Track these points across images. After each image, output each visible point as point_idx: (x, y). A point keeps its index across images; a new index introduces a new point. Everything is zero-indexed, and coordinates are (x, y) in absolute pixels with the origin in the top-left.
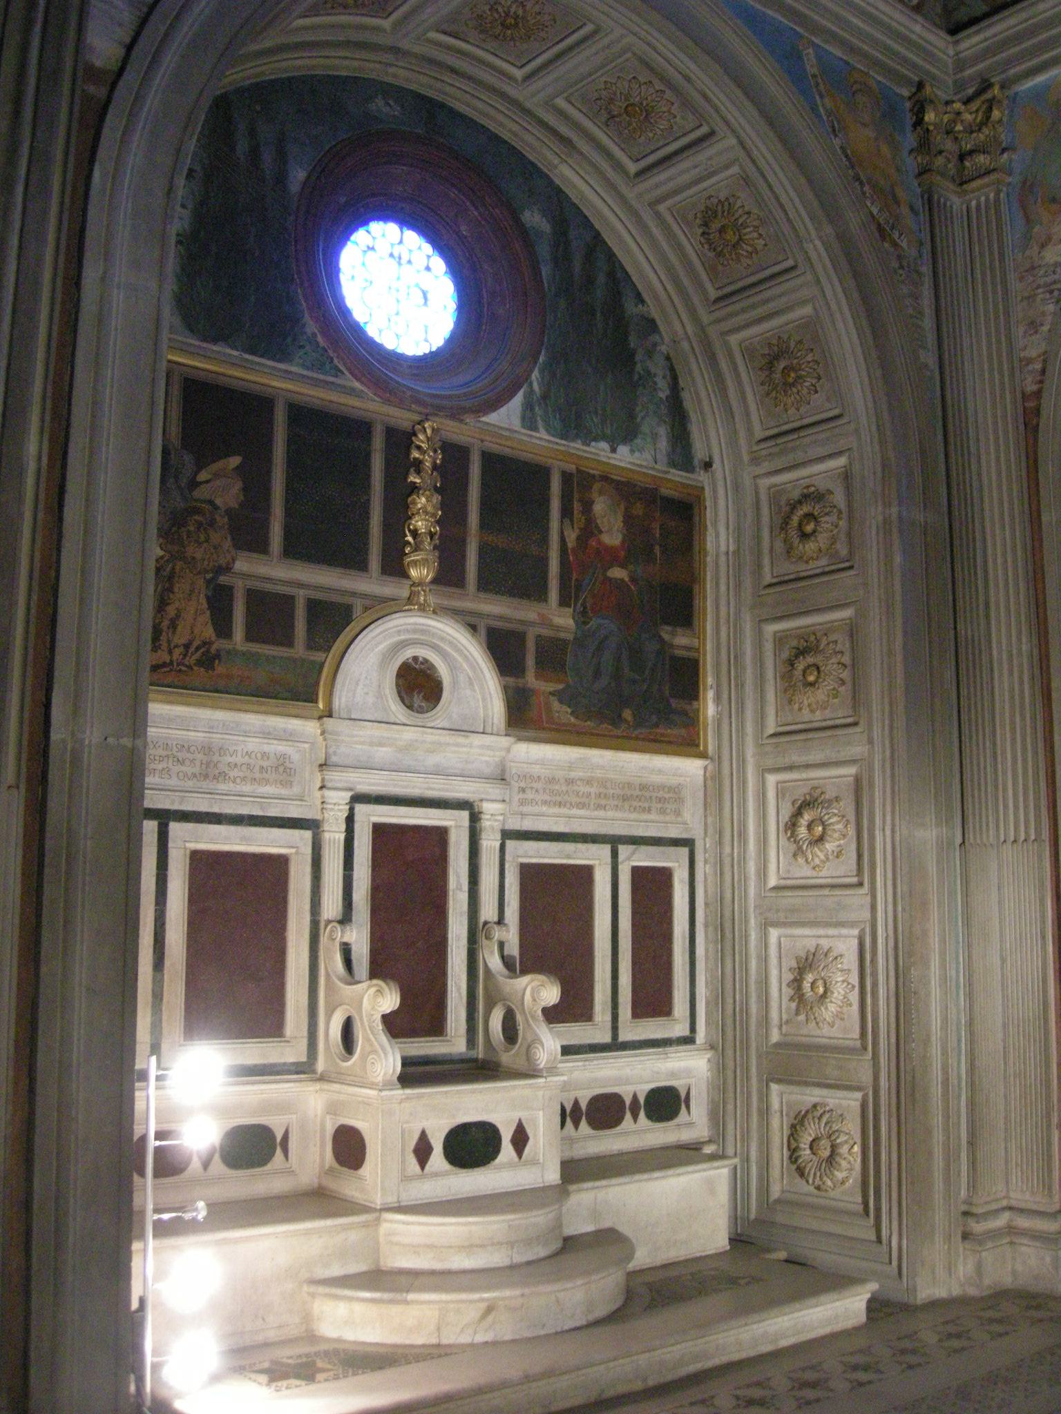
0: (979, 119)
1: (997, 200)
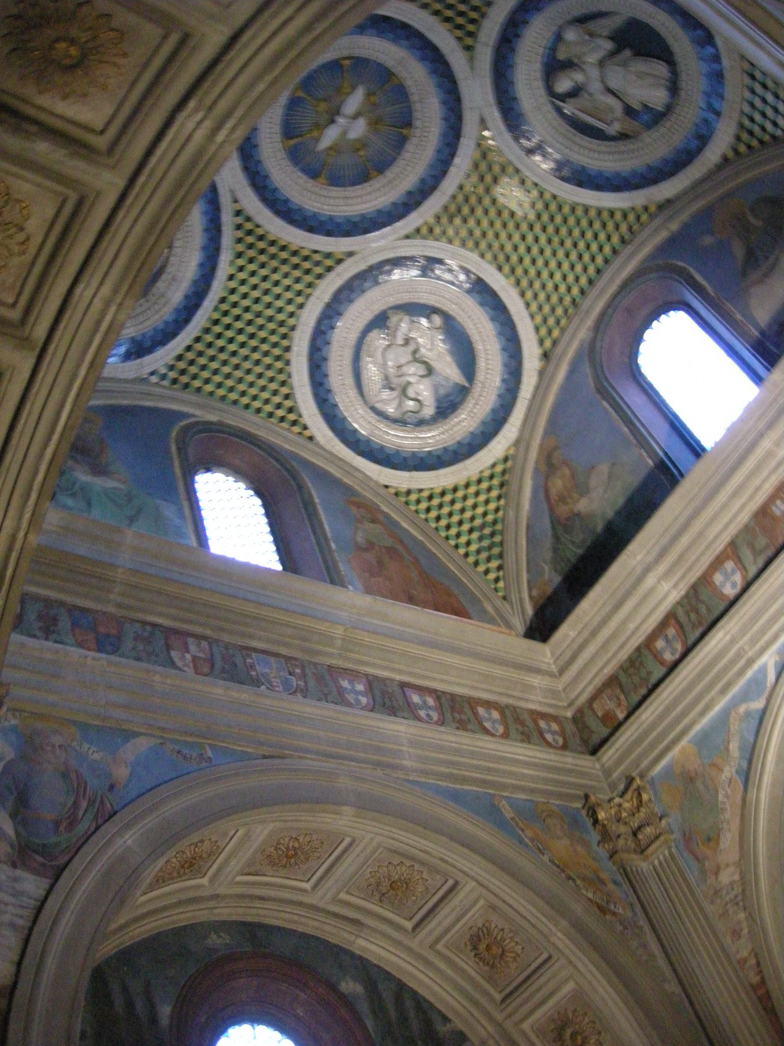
0: (635, 804)
1: (671, 853)
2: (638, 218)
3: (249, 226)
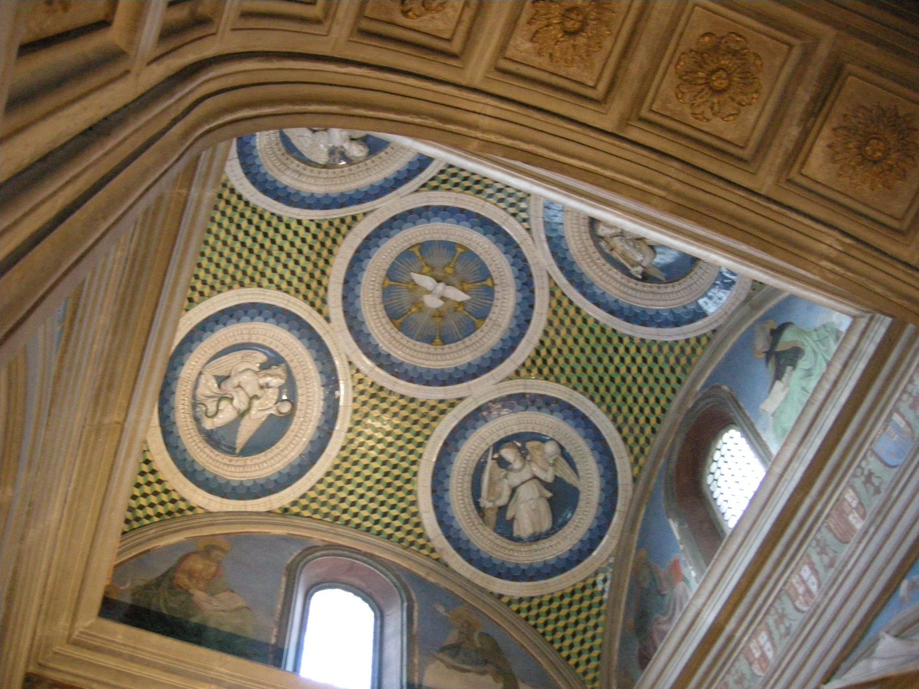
2: (423, 547)
3: (344, 229)
